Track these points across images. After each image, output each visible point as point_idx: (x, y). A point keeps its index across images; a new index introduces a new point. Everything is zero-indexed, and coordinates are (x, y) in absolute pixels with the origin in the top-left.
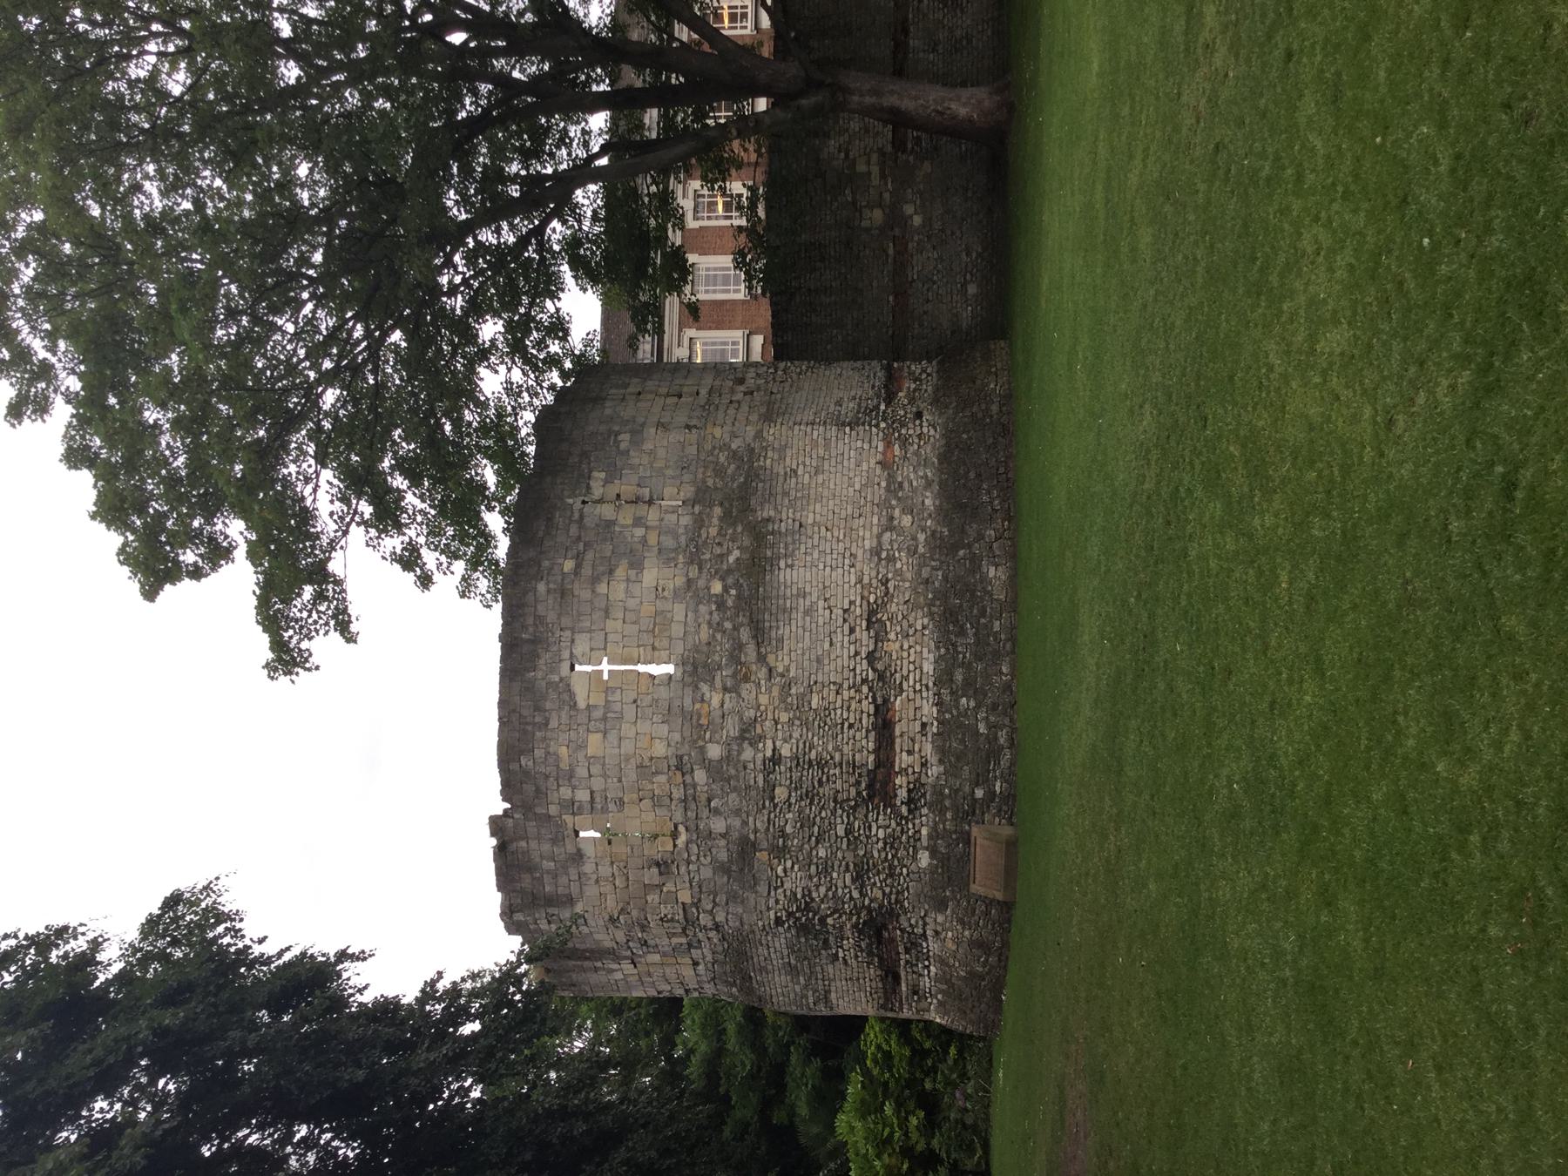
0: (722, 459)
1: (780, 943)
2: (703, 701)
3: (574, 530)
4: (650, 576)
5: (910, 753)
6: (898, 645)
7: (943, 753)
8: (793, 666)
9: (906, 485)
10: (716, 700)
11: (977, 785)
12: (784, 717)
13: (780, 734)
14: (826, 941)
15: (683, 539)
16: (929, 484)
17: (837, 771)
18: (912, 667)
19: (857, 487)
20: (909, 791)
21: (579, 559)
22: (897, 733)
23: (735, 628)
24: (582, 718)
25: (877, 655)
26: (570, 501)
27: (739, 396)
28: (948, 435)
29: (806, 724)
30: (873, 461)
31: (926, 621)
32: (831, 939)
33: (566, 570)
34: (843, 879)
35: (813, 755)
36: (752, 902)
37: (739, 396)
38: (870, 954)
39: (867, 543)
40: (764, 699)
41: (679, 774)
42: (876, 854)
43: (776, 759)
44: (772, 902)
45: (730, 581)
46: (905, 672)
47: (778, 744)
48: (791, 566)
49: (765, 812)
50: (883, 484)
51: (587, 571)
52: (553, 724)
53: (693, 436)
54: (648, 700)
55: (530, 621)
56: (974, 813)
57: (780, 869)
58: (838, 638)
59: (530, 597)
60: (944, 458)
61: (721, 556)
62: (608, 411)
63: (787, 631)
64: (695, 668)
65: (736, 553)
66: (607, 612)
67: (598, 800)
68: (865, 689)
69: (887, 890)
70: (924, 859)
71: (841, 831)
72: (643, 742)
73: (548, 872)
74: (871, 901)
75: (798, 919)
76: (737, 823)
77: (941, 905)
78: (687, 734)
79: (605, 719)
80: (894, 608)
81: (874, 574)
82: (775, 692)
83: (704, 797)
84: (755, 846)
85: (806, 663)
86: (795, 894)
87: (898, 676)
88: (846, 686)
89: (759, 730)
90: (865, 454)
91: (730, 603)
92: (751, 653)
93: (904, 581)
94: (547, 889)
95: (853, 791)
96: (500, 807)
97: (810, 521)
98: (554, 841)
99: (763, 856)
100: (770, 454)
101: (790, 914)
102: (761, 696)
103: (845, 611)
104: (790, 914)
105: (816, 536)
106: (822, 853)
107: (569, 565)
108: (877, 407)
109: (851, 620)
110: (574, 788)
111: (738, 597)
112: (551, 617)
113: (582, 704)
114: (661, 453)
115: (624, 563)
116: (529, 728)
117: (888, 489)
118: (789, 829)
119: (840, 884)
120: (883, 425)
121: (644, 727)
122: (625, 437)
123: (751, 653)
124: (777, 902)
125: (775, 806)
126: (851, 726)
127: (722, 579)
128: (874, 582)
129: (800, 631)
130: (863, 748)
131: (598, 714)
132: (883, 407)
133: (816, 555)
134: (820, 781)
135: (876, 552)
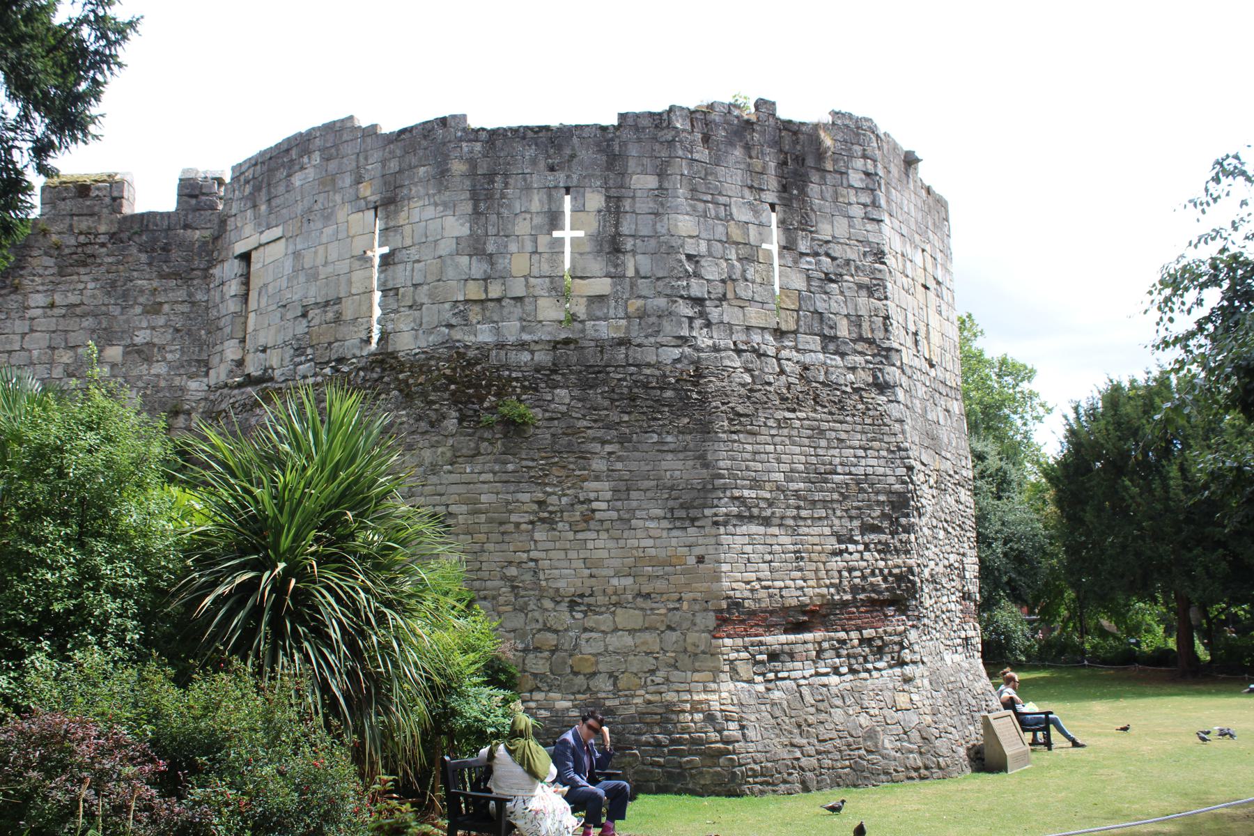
1: (873, 465)
14: (876, 529)
32: (883, 537)
38: (855, 589)
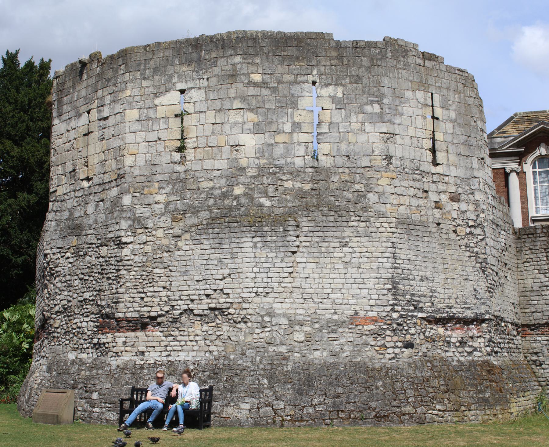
0: (357, 187)
2: (160, 188)
3: (289, 78)
4: (248, 140)
5: (125, 343)
6: (198, 332)
7: (122, 369)
8: (182, 253)
9: (334, 335)
10: (160, 198)
11: (99, 394)
12: (148, 249)
13: (137, 247)
15: (282, 161)
16: (334, 355)
17: (114, 291)
18: (183, 343)
19: (332, 296)
20: (104, 344)
21: (264, 84)
22: (139, 334)
23: (209, 208)
24: (149, 103)
25: (192, 317)
26: (315, 72)
27: (433, 197)
28: (385, 372)
29: (144, 265)
30: (357, 308)
31: (215, 353)
33: (252, 75)
34: (63, 299)
35: (123, 272)
36: (54, 238)
37: (433, 197)
39: (279, 305)
40: (160, 233)
41: (115, 177)
42: (75, 321)
43: (121, 245)
44: (54, 250)
45: (243, 200)
46: (179, 338)
47: (131, 246)
48: (255, 246)
49: (95, 241)
50: (335, 317)
51: (251, 91)
52: (145, 83)
53: (380, 162)
54: (161, 148)
55: (214, 55)
56: (87, 392)
57: (68, 254)
58: (201, 286)
59: (230, 52)
60: (357, 367)
61: (266, 192)
62: (409, 94)
63: (206, 247)
64: (182, 181)
65: (268, 203)
66: (220, 110)
67: (104, 123)
68: (167, 308)
69: (59, 330)
70: (71, 356)
71: (87, 295)
72: (133, 149)
73: (72, 97)
74: (54, 319)
75: (46, 268)
76: (91, 222)
77: (49, 370)
78: (138, 179)
79: (149, 119)
80: (225, 328)
81: (250, 311)
82: (165, 241)
83: (104, 196)
84: (79, 235)
85: (184, 263)
86: (57, 266)
87: (176, 333)
88: (169, 293)
89: (139, 231)
90: (365, 301)
91: (227, 202)
92: (192, 220)
93: (245, 335)
94: (65, 98)
95: (104, 303)
96: (104, 56)
97: (298, 260)
98: (85, 97)
99: (74, 241)
100: (363, 224)
101: (48, 263)
102: (162, 230)
103: (222, 290)
104: (48, 263)
105: (284, 265)
106: (76, 283)
107: (257, 77)
108: (421, 310)
109: (216, 295)
110: (109, 104)
111: (231, 208)
112: (216, 70)
113: (157, 101)
114: (362, 138)
115: (261, 118)
116: (142, 67)
117: (329, 321)
118: (88, 258)
119: (62, 297)
120: (395, 315)
121: (143, 148)
122: (376, 108)
123: (192, 220)
124: (54, 254)
125: (98, 247)
126: (142, 298)
127: (245, 194)
128: (244, 312)
129: (207, 257)
130: (127, 310)
131: (151, 113)
132: (420, 315)
133: (265, 265)
134: (109, 278)
135: (270, 313)
